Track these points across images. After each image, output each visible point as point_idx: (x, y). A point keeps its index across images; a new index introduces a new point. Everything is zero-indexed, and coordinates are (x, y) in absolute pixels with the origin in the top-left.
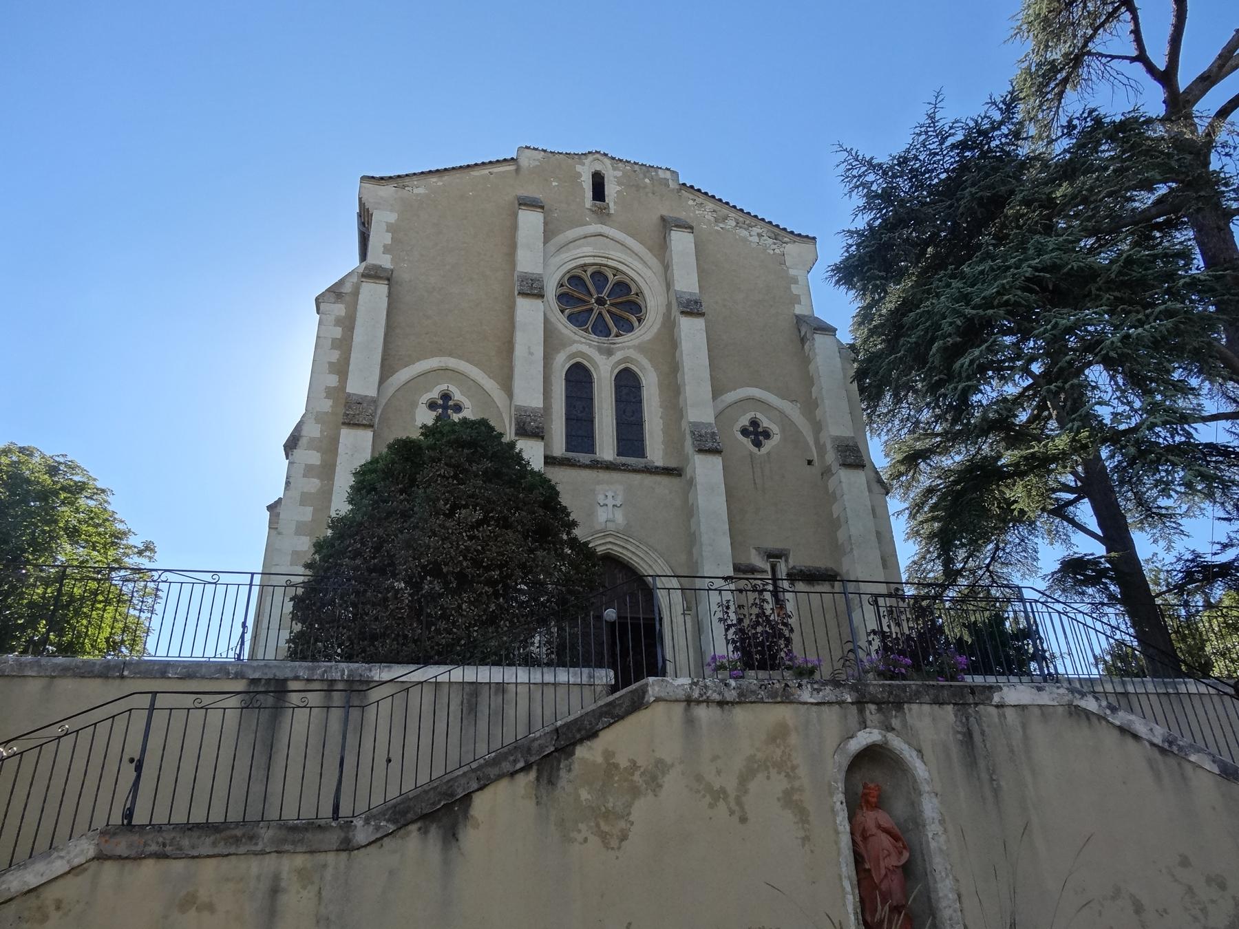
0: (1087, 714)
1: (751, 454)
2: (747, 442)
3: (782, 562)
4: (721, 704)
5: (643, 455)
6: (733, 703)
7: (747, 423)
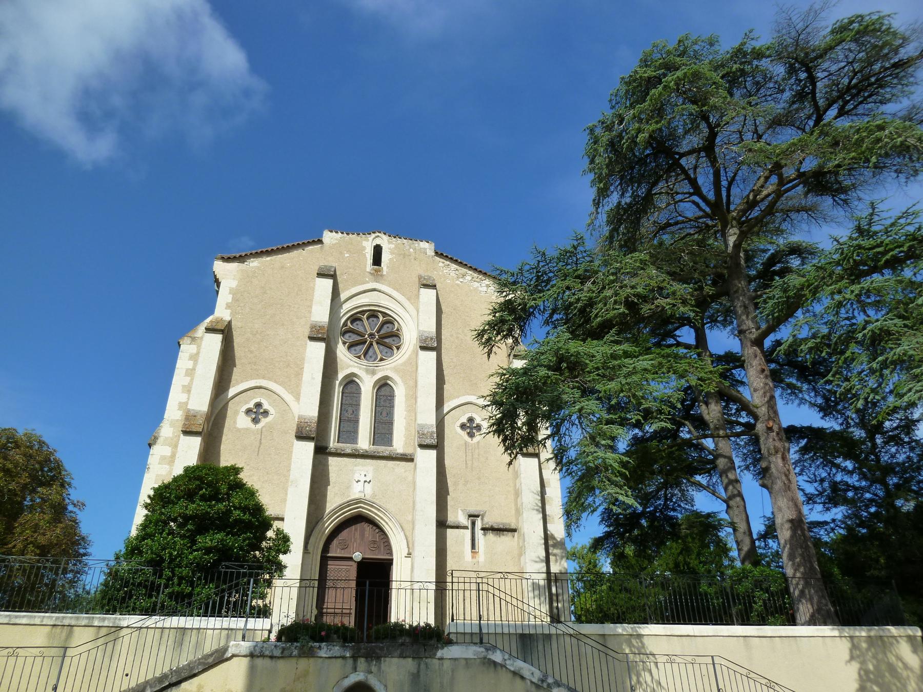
0: (495, 664)
1: (466, 443)
2: (464, 434)
3: (479, 519)
4: (272, 657)
5: (391, 446)
6: (279, 658)
7: (465, 421)
